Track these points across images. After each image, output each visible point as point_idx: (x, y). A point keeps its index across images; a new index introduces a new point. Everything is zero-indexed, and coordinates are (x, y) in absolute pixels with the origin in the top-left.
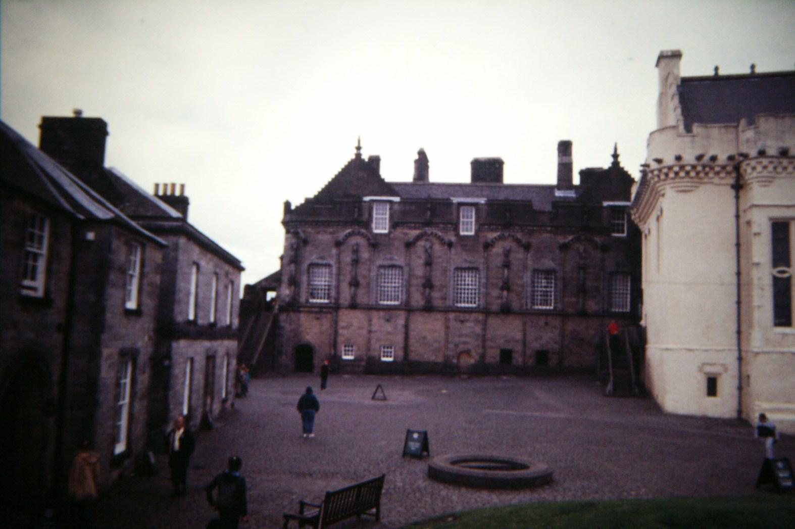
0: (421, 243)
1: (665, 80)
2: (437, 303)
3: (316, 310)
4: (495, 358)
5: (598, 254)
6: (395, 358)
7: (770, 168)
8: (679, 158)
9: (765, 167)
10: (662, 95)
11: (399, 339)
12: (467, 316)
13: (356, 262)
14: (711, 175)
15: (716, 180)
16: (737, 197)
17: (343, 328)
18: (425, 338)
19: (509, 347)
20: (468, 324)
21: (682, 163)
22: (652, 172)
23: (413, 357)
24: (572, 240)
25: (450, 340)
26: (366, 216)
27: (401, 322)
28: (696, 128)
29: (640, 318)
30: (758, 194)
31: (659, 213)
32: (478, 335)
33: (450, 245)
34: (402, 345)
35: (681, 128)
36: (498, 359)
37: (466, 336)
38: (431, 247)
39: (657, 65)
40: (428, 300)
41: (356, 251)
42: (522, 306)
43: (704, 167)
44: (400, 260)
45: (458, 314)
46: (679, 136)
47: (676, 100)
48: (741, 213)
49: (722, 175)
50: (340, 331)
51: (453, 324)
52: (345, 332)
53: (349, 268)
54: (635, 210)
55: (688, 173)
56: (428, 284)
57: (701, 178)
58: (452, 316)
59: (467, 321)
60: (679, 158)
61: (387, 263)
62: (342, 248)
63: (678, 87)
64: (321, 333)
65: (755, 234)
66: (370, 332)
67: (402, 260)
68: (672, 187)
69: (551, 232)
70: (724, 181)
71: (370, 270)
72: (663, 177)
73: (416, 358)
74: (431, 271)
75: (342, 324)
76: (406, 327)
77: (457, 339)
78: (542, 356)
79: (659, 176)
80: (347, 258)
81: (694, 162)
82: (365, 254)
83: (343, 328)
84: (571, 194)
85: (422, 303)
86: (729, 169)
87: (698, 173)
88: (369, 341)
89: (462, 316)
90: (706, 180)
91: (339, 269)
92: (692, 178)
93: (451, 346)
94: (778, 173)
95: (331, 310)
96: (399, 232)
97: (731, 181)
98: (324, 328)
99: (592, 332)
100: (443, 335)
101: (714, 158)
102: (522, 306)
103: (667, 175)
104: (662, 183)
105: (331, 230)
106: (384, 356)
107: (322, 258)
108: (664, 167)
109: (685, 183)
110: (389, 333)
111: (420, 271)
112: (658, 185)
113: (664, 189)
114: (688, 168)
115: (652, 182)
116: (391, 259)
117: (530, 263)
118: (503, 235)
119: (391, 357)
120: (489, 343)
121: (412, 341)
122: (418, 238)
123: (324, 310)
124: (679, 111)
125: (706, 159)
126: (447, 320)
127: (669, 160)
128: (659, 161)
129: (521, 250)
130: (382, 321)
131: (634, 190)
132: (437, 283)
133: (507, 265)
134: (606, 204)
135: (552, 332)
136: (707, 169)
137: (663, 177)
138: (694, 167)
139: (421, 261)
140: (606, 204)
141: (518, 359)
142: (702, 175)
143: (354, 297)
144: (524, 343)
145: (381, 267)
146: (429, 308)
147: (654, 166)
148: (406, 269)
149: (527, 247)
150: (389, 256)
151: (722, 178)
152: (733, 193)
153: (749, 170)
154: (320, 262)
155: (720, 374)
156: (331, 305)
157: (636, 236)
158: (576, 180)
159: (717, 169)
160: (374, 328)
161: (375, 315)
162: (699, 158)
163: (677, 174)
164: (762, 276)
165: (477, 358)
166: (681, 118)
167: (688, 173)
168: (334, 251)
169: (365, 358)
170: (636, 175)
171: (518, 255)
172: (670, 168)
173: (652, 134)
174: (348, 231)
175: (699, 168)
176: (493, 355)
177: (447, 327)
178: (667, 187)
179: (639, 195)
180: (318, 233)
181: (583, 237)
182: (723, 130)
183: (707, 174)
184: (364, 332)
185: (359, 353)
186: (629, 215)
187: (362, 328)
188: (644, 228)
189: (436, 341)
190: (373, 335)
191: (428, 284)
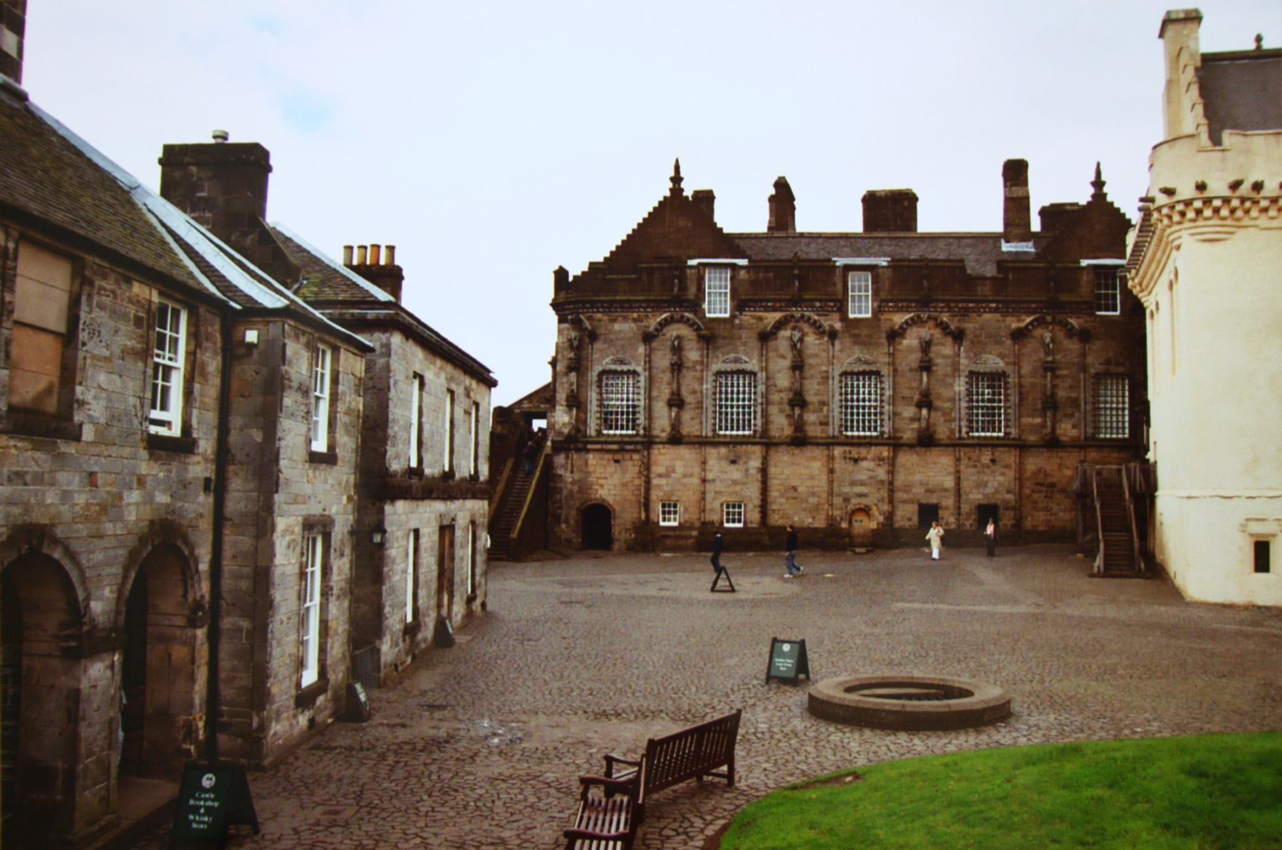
0: (786, 333)
1: (1174, 59)
2: (814, 431)
3: (615, 447)
4: (910, 519)
5: (1073, 346)
6: (745, 523)
8: (1201, 187)
10: (1170, 84)
11: (752, 492)
12: (863, 451)
13: (677, 367)
14: (1254, 213)
15: (1263, 221)
17: (660, 476)
18: (795, 489)
20: (864, 464)
21: (1207, 194)
22: (1159, 209)
23: (775, 519)
24: (1031, 323)
25: (836, 490)
26: (692, 290)
27: (755, 463)
28: (1228, 137)
29: (1147, 449)
31: (1172, 276)
32: (882, 482)
33: (833, 335)
34: (757, 502)
35: (1204, 138)
36: (915, 518)
37: (862, 484)
38: (801, 340)
39: (1161, 36)
40: (799, 426)
41: (677, 349)
42: (952, 432)
43: (1243, 200)
44: (752, 364)
46: (1202, 150)
47: (1195, 90)
49: (1273, 213)
50: (655, 481)
51: (838, 465)
52: (663, 481)
53: (667, 377)
54: (1133, 272)
55: (1216, 211)
56: (798, 400)
57: (1238, 220)
58: (838, 451)
59: (865, 459)
60: (1201, 187)
61: (729, 367)
62: (654, 345)
63: (1197, 69)
64: (624, 485)
66: (704, 481)
67: (754, 361)
68: (1193, 235)
69: (996, 310)
71: (701, 381)
72: (1176, 218)
73: (781, 522)
74: (802, 378)
75: (656, 469)
76: (764, 471)
77: (846, 489)
79: (1170, 217)
80: (663, 360)
81: (1227, 193)
82: (693, 354)
83: (660, 476)
84: (1028, 247)
85: (788, 431)
87: (1233, 211)
89: (855, 452)
90: (1246, 222)
91: (650, 380)
92: (1224, 219)
93: (838, 501)
95: (639, 447)
96: (747, 317)
98: (628, 476)
99: (1068, 473)
101: (1258, 187)
102: (952, 432)
103: (1183, 214)
104: (1176, 228)
105: (635, 315)
106: (728, 521)
107: (622, 362)
108: (1179, 202)
109: (1210, 226)
110: (735, 482)
111: (783, 380)
112: (1169, 231)
113: (1180, 237)
114: (1217, 203)
115: (1159, 226)
116: (737, 360)
117: (964, 361)
118: (919, 317)
119: (739, 521)
120: (899, 495)
121: (774, 494)
122: (779, 325)
123: (628, 447)
124: (1200, 109)
125: (1245, 189)
126: (831, 458)
127: (1186, 191)
128: (1169, 192)
130: (724, 464)
131: (1131, 238)
132: (811, 397)
133: (926, 366)
134: (1084, 263)
135: (1003, 474)
136: (1248, 204)
137: (1176, 218)
138: (1226, 201)
139: (787, 363)
140: (1084, 263)
142: (1239, 213)
143: (676, 425)
145: (719, 373)
146: (800, 440)
147: (1162, 199)
148: (761, 376)
149: (958, 337)
150: (732, 356)
151: (1273, 218)
154: (619, 368)
155: (1274, 536)
156: (638, 439)
157: (1136, 313)
158: (1036, 225)
159: (1264, 203)
160: (710, 476)
161: (712, 452)
162: (1235, 186)
163: (1199, 212)
165: (881, 518)
166: (1204, 121)
167: (1216, 211)
168: (641, 349)
169: (697, 524)
170: (1134, 216)
171: (944, 350)
172: (1188, 203)
173: (1155, 147)
175: (1235, 203)
177: (832, 471)
178: (1184, 234)
179: (1138, 247)
180: (614, 321)
181: (1049, 319)
182: (1272, 139)
183: (1247, 212)
184: (696, 481)
185: (687, 516)
186: (1124, 281)
187: (691, 476)
188: (1148, 302)
189: (813, 494)
190: (708, 485)
191: (798, 400)
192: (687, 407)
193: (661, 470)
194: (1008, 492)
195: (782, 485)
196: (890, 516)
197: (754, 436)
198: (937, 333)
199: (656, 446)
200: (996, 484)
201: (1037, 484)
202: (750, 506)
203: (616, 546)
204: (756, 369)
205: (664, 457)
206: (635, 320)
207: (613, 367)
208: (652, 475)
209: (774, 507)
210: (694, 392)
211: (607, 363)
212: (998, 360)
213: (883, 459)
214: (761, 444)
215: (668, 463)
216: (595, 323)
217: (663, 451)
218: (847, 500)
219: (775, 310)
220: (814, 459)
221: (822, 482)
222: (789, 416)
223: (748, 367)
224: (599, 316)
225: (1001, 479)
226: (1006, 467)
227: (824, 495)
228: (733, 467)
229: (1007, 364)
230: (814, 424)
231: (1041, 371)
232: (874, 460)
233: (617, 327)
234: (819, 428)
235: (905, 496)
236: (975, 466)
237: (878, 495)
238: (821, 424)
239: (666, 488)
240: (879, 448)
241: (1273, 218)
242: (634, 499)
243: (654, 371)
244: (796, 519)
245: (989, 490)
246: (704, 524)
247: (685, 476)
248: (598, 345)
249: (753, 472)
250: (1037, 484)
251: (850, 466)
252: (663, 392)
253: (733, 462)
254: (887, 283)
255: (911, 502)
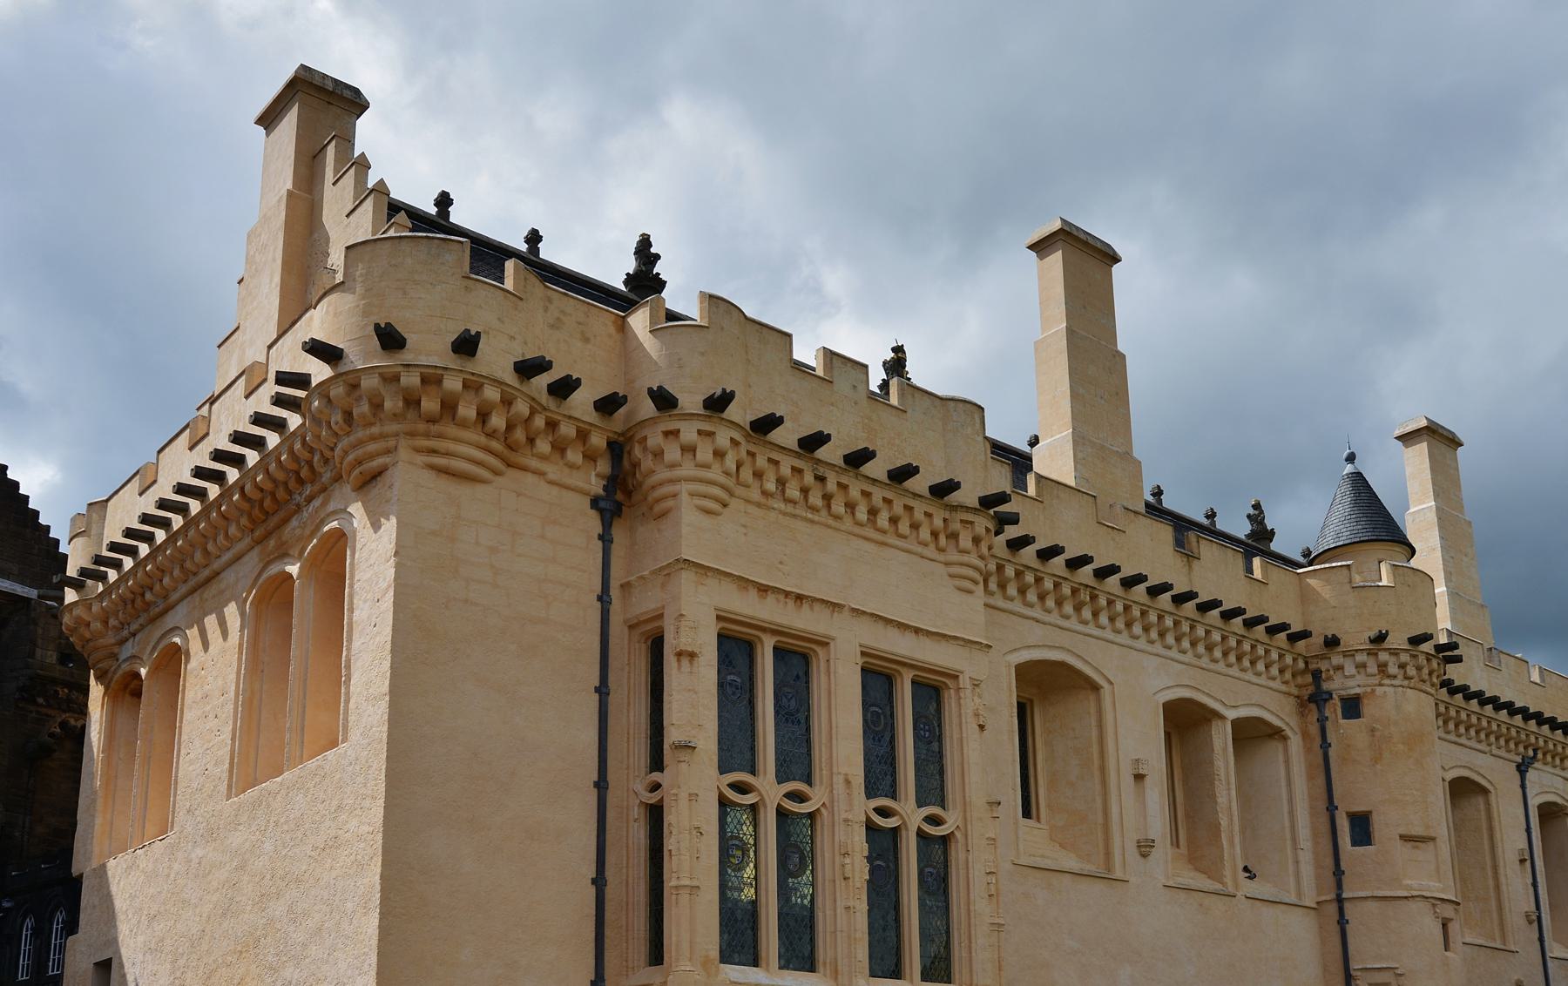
7: (730, 463)
9: (719, 454)
15: (553, 470)
16: (606, 539)
30: (693, 531)
48: (615, 592)
65: (679, 654)
70: (576, 480)
86: (598, 441)
94: (739, 483)
97: (596, 486)
152: (594, 523)
153: (672, 453)
164: (695, 787)
241: (572, 466)
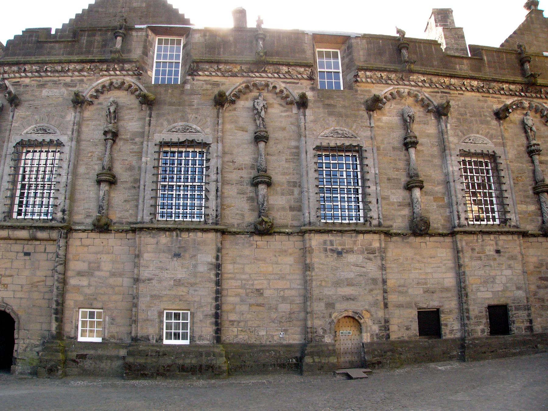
3: (24, 234)
4: (407, 329)
6: (192, 339)
11: (204, 294)
12: (347, 241)
13: (113, 136)
17: (80, 274)
18: (259, 292)
19: (433, 303)
20: (351, 258)
23: (233, 334)
25: (316, 292)
27: (207, 257)
34: (210, 310)
36: (415, 326)
37: (350, 283)
38: (265, 108)
40: (261, 210)
41: (114, 115)
45: (325, 237)
50: (73, 281)
51: (318, 259)
52: (84, 282)
53: (99, 150)
56: (261, 179)
59: (350, 251)
61: (175, 138)
62: (87, 114)
64: (33, 285)
66: (137, 280)
67: (208, 130)
71: (139, 154)
73: (243, 338)
75: (75, 266)
77: (329, 291)
78: (499, 317)
80: (94, 127)
82: (131, 123)
83: (80, 274)
85: (251, 218)
88: (134, 301)
89: (337, 240)
91: (78, 152)
95: (54, 234)
98: (41, 274)
100: (297, 284)
105: (68, 80)
106: (169, 336)
107: (45, 131)
110: (178, 283)
111: (244, 155)
116: (185, 130)
117: (452, 139)
119: (185, 337)
120: (393, 298)
121: (230, 300)
123: (40, 234)
126: (305, 251)
129: (432, 118)
130: (165, 257)
132: (277, 177)
135: (510, 267)
139: (248, 136)
141: (451, 327)
143: (103, 207)
144: (462, 291)
145: (163, 144)
146: (263, 229)
149: (441, 112)
150: (180, 124)
154: (40, 138)
156: (54, 224)
160: (145, 274)
161: (148, 241)
165: (376, 328)
168: (71, 116)
174: (105, 80)
176: (404, 325)
180: (42, 86)
184: (127, 282)
185: (114, 330)
187: (121, 275)
189: (284, 299)
190: (141, 286)
191: (261, 179)
192: (120, 186)
193: (81, 266)
194: (518, 288)
195: (243, 287)
196: (386, 325)
197: (205, 222)
198: (417, 111)
199: (75, 235)
200: (504, 280)
201: (541, 279)
202: (199, 316)
203: (18, 368)
204: (209, 140)
205: (85, 248)
206: (66, 85)
207: (34, 137)
208: (69, 273)
209: (233, 317)
210: (131, 168)
211: (27, 132)
212: (487, 140)
213: (373, 252)
214: (216, 231)
215: (92, 257)
216: (22, 89)
217: (87, 242)
218: (330, 305)
219: (235, 75)
220: (284, 252)
221: (292, 285)
222: (251, 199)
223: (199, 137)
224: (27, 81)
225: (508, 272)
226: (512, 258)
227: (299, 300)
228: (176, 263)
229: (496, 144)
230: (283, 209)
231: (526, 157)
232: (362, 253)
233: (45, 92)
234: (290, 214)
235: (402, 299)
236: (480, 259)
237: (370, 298)
238: (292, 209)
239: (88, 291)
240: (368, 237)
242: (44, 303)
243: (84, 144)
244: (262, 333)
245: (498, 288)
246: (135, 339)
247: (113, 275)
248: (20, 112)
249: (202, 268)
250: (541, 279)
251: (331, 260)
252: (91, 168)
253: (177, 255)
254: (361, 53)
255: (408, 306)
